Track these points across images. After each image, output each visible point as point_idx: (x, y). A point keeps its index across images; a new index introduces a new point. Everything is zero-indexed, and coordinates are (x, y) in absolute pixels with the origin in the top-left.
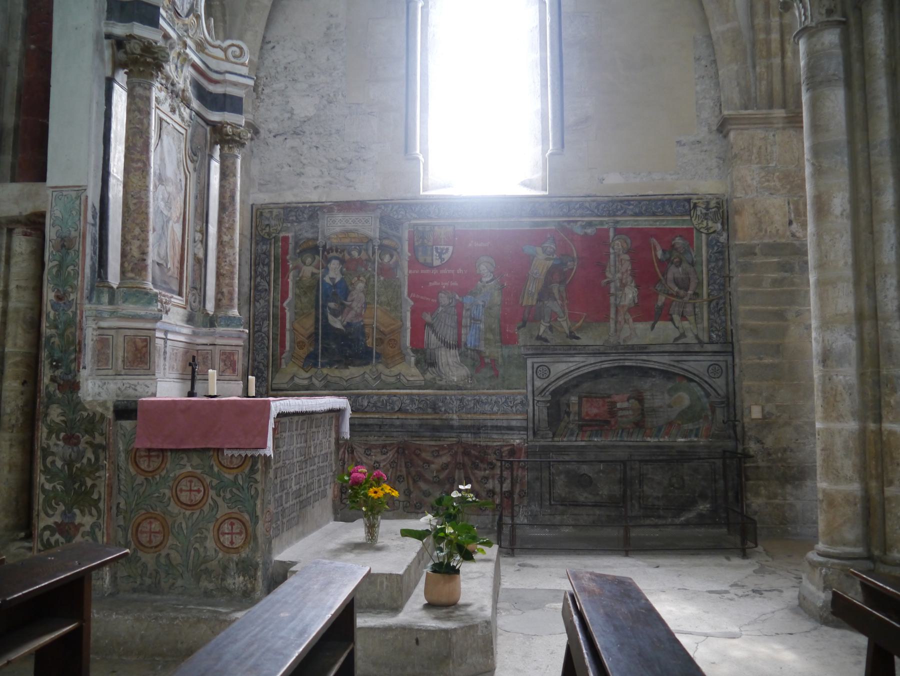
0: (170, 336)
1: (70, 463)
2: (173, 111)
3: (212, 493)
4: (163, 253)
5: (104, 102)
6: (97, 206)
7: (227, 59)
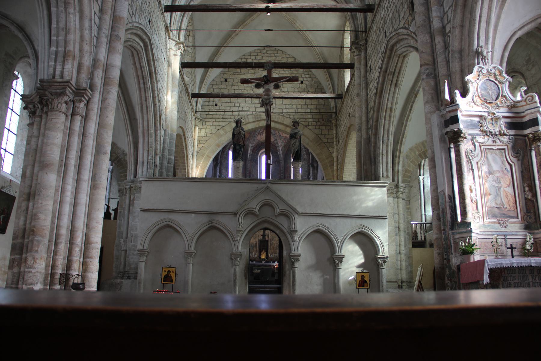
0: (508, 237)
2: (494, 142)
4: (499, 202)
5: (449, 157)
6: (451, 195)
7: (527, 104)
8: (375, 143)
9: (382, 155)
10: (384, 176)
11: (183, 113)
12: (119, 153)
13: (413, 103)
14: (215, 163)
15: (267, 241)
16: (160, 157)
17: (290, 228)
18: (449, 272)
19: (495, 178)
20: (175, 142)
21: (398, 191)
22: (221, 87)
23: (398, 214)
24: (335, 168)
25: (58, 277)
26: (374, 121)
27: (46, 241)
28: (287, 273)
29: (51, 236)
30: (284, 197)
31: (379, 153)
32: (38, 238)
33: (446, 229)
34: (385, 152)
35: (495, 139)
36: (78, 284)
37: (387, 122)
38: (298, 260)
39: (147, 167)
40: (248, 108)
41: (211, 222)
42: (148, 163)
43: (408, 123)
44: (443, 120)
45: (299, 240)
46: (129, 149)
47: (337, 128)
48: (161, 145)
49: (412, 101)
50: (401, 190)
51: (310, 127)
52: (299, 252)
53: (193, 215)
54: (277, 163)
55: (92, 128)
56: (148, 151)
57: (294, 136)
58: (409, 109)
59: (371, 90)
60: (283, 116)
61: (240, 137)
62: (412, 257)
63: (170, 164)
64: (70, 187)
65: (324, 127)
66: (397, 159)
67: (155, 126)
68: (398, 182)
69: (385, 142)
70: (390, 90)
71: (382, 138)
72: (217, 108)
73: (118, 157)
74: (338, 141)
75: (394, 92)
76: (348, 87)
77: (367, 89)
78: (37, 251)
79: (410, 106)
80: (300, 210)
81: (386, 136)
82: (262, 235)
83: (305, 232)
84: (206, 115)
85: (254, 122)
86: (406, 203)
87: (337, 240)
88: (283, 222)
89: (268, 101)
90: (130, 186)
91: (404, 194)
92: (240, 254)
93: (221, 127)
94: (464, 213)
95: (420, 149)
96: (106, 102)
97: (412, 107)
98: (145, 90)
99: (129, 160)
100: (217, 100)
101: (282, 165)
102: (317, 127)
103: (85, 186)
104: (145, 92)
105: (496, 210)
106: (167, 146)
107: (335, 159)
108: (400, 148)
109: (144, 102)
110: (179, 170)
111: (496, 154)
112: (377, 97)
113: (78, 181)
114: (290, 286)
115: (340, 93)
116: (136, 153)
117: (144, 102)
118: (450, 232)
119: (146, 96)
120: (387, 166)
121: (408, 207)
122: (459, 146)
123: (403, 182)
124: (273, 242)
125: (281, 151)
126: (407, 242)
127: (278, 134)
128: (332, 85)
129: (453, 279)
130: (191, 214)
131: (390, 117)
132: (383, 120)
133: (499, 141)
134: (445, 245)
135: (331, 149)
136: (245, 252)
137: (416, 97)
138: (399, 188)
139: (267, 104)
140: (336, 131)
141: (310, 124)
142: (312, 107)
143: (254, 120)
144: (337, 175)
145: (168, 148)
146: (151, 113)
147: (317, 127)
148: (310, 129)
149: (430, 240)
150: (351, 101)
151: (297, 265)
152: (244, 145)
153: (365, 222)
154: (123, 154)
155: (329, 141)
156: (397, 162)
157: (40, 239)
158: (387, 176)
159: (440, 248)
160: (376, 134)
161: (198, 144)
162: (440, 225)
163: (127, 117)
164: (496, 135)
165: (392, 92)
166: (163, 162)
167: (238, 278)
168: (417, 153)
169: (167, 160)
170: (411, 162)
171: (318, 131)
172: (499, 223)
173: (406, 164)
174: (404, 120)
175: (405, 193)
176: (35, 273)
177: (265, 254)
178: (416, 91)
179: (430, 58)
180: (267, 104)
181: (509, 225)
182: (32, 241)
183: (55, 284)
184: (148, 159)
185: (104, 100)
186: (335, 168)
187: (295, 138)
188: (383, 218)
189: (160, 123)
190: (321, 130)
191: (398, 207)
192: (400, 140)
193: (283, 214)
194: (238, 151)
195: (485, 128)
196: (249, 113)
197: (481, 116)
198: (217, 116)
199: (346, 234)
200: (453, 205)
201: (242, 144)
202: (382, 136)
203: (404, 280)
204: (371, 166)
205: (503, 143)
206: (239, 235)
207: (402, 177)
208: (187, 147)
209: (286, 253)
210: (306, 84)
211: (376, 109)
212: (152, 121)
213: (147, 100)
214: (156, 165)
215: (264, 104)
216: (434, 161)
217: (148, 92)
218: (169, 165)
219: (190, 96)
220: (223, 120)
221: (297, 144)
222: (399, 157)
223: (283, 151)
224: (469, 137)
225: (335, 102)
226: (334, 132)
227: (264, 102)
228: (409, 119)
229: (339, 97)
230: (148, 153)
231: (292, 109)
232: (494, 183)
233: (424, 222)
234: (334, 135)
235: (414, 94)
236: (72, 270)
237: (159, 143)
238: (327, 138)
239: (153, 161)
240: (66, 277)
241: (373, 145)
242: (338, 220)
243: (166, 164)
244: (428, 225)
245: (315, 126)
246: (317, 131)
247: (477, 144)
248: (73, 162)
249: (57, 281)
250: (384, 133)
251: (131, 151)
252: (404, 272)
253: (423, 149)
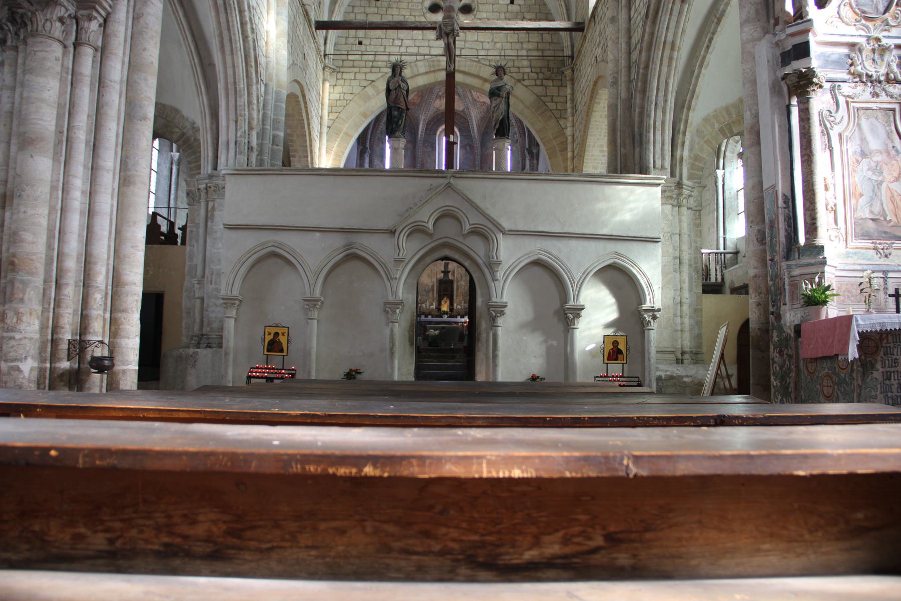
0: (890, 275)
1: (781, 367)
2: (875, 95)
3: (836, 387)
4: (877, 209)
5: (787, 123)
6: (789, 195)
8: (642, 108)
9: (655, 128)
10: (657, 166)
11: (301, 56)
12: (185, 128)
13: (714, 33)
14: (362, 147)
15: (452, 282)
16: (258, 134)
17: (488, 256)
18: (778, 336)
19: (873, 164)
20: (284, 106)
21: (680, 194)
22: (368, 10)
23: (680, 235)
24: (569, 154)
25: (64, 346)
26: (642, 66)
27: (38, 281)
28: (484, 335)
29: (48, 272)
30: (478, 201)
31: (649, 125)
32: (21, 276)
33: (777, 258)
34: (659, 124)
35: (878, 90)
36: (102, 359)
37: (665, 69)
38: (502, 313)
39: (236, 152)
40: (417, 48)
41: (349, 246)
42: (236, 143)
43: (703, 71)
44: (778, 52)
45: (504, 278)
46: (202, 120)
47: (573, 84)
48: (259, 111)
49: (711, 31)
50: (686, 192)
51: (526, 83)
52: (505, 299)
53: (318, 234)
54: (468, 148)
55: (117, 70)
56: (236, 122)
57: (498, 92)
58: (705, 45)
59: (637, 10)
60: (479, 62)
61: (400, 93)
62: (701, 310)
63: (277, 145)
64: (79, 183)
65: (550, 83)
66: (681, 136)
67: (247, 76)
68: (681, 178)
69: (660, 105)
70: (672, 9)
71: (654, 98)
72: (362, 48)
73: (183, 134)
74: (575, 107)
75: (680, 13)
76: (595, 8)
77: (630, 10)
78: (22, 300)
79: (707, 39)
80: (506, 225)
81: (661, 94)
82: (442, 272)
83: (515, 264)
84: (343, 60)
85: (427, 73)
86: (694, 215)
87: (572, 279)
88: (476, 246)
89: (449, 28)
90: (207, 184)
91: (691, 200)
92: (401, 303)
93: (370, 82)
94: (812, 228)
95: (722, 120)
96: (142, 21)
97: (710, 41)
98: (226, 9)
99: (204, 139)
100: (361, 33)
101: (478, 151)
102: (539, 82)
103: (109, 181)
104: (227, 13)
105: (871, 224)
106: (270, 113)
107: (570, 139)
108: (687, 116)
109: (225, 32)
110: (296, 159)
111: (876, 118)
112: (649, 23)
113: (94, 169)
114: (487, 358)
115: (579, 20)
116: (215, 126)
117: (225, 32)
118: (784, 264)
119: (228, 21)
120: (662, 149)
121: (698, 222)
122: (807, 101)
123: (690, 178)
124: (461, 283)
125: (475, 128)
126: (694, 284)
127: (470, 98)
128: (566, 6)
129: (786, 351)
130: (314, 233)
131: (671, 59)
132: (658, 66)
133: (883, 94)
134: (772, 288)
135: (562, 122)
136: (410, 300)
137: (718, 23)
138: (682, 188)
139: (447, 35)
140: (573, 89)
141: (526, 77)
142: (530, 46)
143: (428, 70)
144: (572, 167)
145: (272, 117)
146: (239, 52)
147: (539, 82)
148: (526, 86)
149: (732, 282)
150: (600, 33)
151: (500, 321)
152: (408, 109)
153: (620, 247)
154: (193, 128)
155: (559, 107)
156: (680, 141)
157: (25, 278)
158: (663, 167)
159: (760, 293)
160: (644, 91)
161: (329, 113)
162: (764, 251)
163: (196, 61)
164: (880, 82)
165: (675, 13)
166: (264, 142)
167: (397, 344)
168: (717, 126)
169: (271, 137)
170: (705, 142)
171: (541, 88)
172: (875, 249)
173: (697, 146)
174: (695, 66)
175: (693, 198)
176: (20, 339)
177: (448, 303)
178: (719, 12)
180: (447, 35)
181: (894, 252)
182: (12, 282)
183: (60, 360)
184: (236, 137)
186: (569, 154)
187: (499, 96)
188: (654, 240)
189: (257, 72)
190: (546, 87)
191: (680, 222)
192: (687, 102)
193: (474, 232)
194: (395, 120)
195: (859, 68)
196: (419, 58)
197: (852, 46)
198: (363, 64)
199: (587, 269)
200: (791, 214)
201: (404, 107)
202: (655, 94)
203: (687, 349)
204: (634, 148)
205: (892, 97)
206: (398, 270)
207: (688, 169)
208: (310, 117)
209: (483, 301)
210: (519, 5)
211: (645, 45)
212: (241, 67)
213: (231, 28)
214: (252, 148)
215: (443, 34)
216: (758, 134)
217: (231, 13)
218: (275, 147)
219: (313, 26)
220: (373, 70)
221: (503, 106)
222: (684, 133)
223: (479, 127)
224: (827, 86)
225: (571, 37)
226: (569, 91)
227: (443, 31)
228: (705, 64)
229: (579, 28)
230: (236, 126)
231: (494, 49)
232: (870, 173)
233: (722, 250)
234: (569, 97)
235: (715, 17)
236: (90, 333)
237: (255, 107)
238: (556, 103)
239: (246, 141)
240: (79, 346)
241: (637, 110)
242: (573, 243)
243: (270, 146)
244: (728, 256)
245: (535, 80)
246: (539, 90)
247: (842, 100)
248: (82, 135)
249: (63, 354)
250: (658, 89)
251: (206, 124)
252: (687, 335)
253: (727, 119)
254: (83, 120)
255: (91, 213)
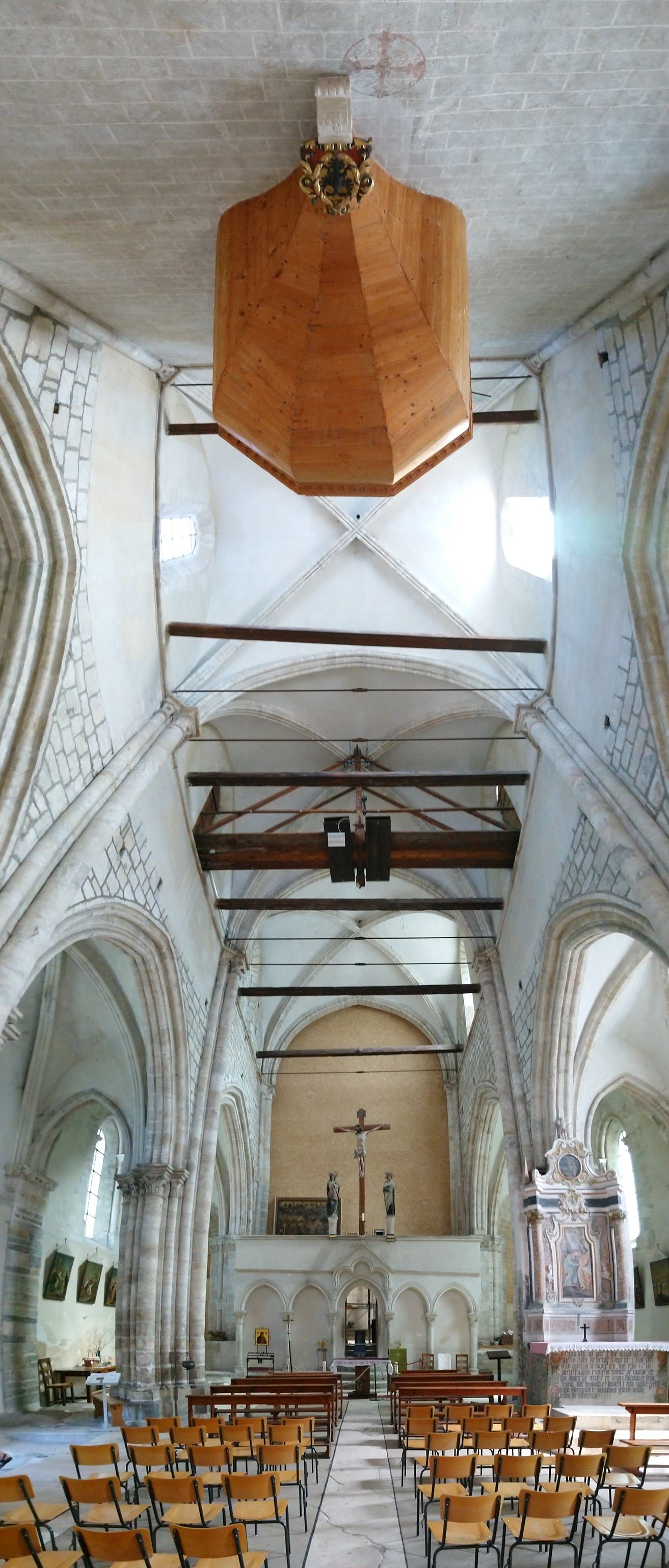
4: (575, 1281)
27: (152, 1323)
29: (156, 1318)
55: (190, 1208)
64: (171, 1270)
78: (145, 1334)
105: (572, 1289)
113: (179, 1262)
179: (513, 1127)
185: (200, 1178)
240: (175, 1356)
248: (173, 1244)
254: (173, 1237)
255: (177, 1285)
